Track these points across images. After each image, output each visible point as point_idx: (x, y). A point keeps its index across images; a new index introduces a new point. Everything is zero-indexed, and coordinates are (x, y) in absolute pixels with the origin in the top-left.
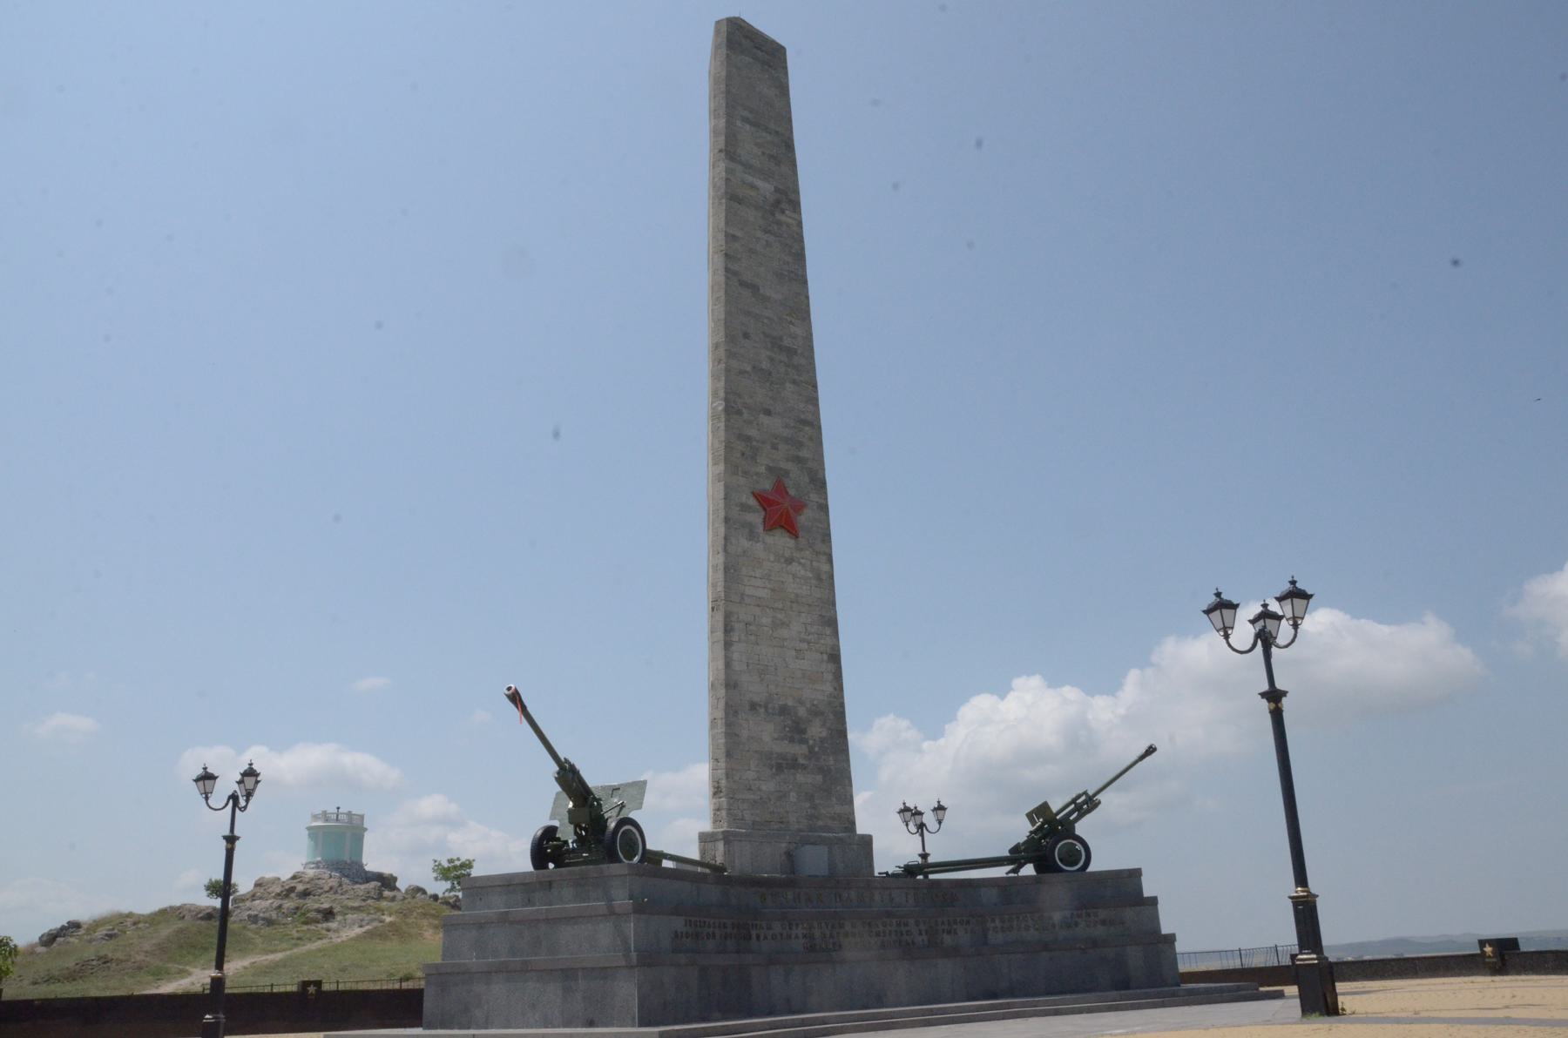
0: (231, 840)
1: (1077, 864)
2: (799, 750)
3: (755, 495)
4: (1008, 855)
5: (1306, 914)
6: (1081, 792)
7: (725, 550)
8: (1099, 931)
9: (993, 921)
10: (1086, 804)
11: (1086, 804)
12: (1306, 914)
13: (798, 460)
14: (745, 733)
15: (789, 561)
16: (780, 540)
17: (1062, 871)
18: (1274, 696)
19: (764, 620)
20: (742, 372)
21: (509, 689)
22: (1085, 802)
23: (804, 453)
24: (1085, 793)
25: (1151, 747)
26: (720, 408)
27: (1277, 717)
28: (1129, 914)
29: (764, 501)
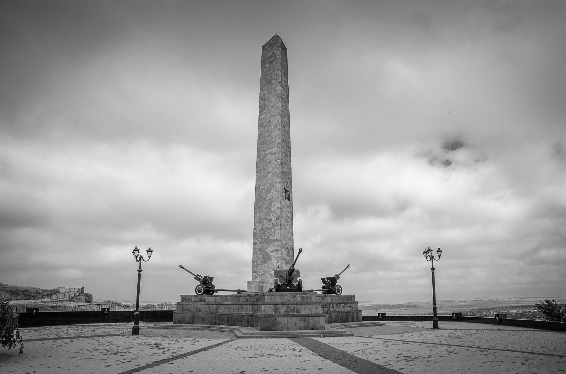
0: (140, 271)
1: (339, 292)
2: (289, 258)
3: (284, 188)
4: (322, 289)
5: (435, 310)
6: (336, 274)
7: (281, 204)
8: (349, 309)
9: (331, 305)
10: (338, 277)
11: (338, 277)
12: (435, 310)
13: (289, 178)
14: (283, 254)
15: (288, 208)
16: (287, 201)
17: (337, 294)
18: (433, 269)
19: (285, 223)
20: (283, 152)
21: (301, 249)
22: (337, 278)
23: (290, 177)
24: (337, 275)
25: (349, 265)
26: (280, 162)
27: (433, 273)
28: (353, 305)
29: (286, 191)
